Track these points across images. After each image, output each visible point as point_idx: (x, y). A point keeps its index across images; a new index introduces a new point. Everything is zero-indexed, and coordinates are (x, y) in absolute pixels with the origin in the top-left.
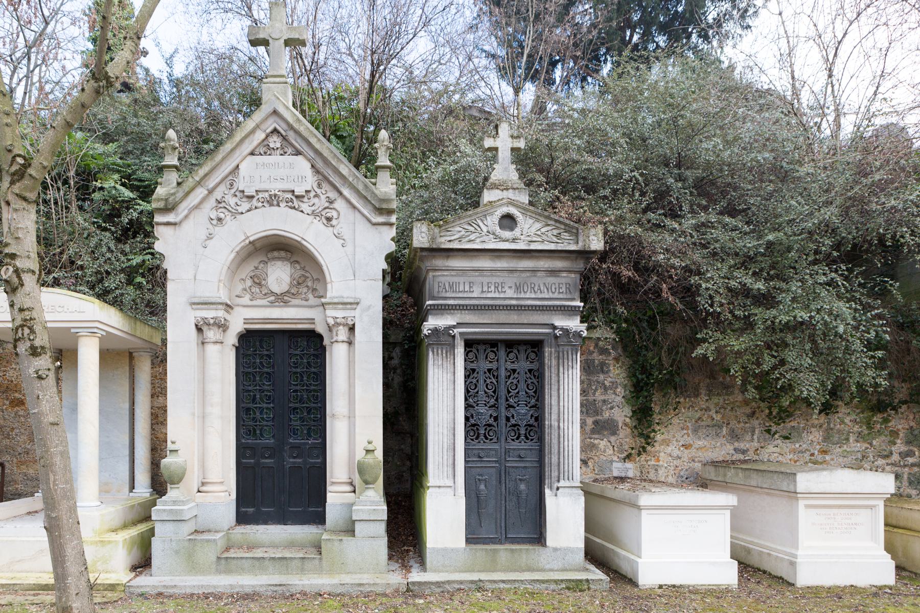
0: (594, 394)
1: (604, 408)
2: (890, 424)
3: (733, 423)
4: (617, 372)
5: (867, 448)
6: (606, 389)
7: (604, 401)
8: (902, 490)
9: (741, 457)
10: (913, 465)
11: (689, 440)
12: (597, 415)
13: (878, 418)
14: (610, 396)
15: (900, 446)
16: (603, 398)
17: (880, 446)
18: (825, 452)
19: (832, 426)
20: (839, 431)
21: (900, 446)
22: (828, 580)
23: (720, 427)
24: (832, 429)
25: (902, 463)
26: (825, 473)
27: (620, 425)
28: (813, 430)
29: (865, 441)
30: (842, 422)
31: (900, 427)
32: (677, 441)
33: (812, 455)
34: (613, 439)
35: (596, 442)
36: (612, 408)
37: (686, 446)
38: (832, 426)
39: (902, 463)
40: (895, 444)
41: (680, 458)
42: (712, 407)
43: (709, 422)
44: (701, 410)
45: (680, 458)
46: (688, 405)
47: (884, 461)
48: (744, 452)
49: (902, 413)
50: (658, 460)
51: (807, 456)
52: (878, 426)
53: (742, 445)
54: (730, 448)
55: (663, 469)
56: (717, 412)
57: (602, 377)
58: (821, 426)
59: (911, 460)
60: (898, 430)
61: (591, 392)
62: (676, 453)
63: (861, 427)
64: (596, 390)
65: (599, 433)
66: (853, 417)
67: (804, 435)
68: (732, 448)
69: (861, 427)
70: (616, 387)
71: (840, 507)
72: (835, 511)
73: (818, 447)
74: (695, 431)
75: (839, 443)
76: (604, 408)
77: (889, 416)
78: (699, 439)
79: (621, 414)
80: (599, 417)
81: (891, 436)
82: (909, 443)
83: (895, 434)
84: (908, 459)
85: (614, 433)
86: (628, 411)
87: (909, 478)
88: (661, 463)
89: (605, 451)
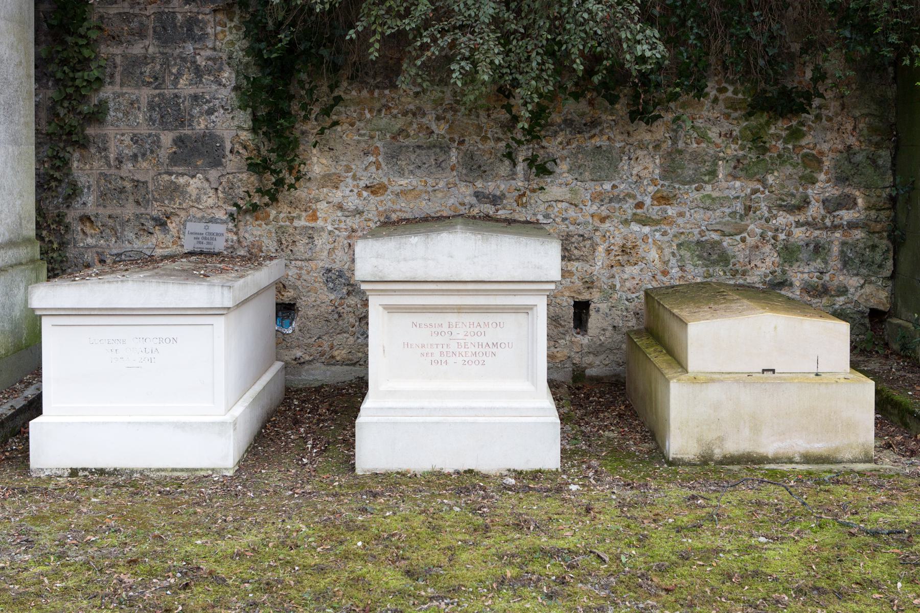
0: (175, 83)
1: (196, 111)
2: (803, 142)
3: (472, 140)
4: (229, 38)
5: (755, 191)
6: (199, 72)
7: (195, 98)
8: (827, 277)
9: (489, 209)
10: (852, 225)
11: (379, 176)
12: (182, 125)
13: (779, 128)
14: (208, 87)
15: (823, 187)
16: (192, 90)
17: (783, 186)
18: (663, 199)
19: (681, 145)
20: (695, 156)
21: (823, 187)
22: (420, 461)
23: (445, 149)
24: (680, 152)
25: (828, 222)
26: (414, 240)
27: (228, 146)
28: (640, 153)
29: (750, 177)
30: (703, 137)
31: (825, 147)
32: (354, 177)
33: (640, 205)
34: (213, 174)
35: (181, 180)
36: (210, 112)
37: (375, 189)
38: (681, 145)
39: (828, 222)
40: (813, 181)
41: (360, 213)
42: (428, 107)
43: (422, 139)
44: (405, 114)
45: (360, 213)
46: (377, 105)
47: (791, 219)
48: (495, 200)
49: (830, 119)
50: (314, 218)
51: (628, 207)
52: (780, 145)
53: (491, 187)
54: (465, 192)
55: (325, 235)
56: (438, 118)
57: (190, 48)
58: (657, 147)
59: (847, 215)
60: (822, 153)
61: (169, 80)
62: (353, 202)
63: (742, 148)
64: (179, 75)
65: (186, 162)
66: (726, 126)
67: (624, 165)
69: (742, 148)
70: (220, 70)
71: (45, 309)
72: (452, 318)
73: (651, 189)
75: (696, 181)
76: (196, 111)
77: (802, 124)
78: (401, 173)
79: (231, 127)
80: (187, 131)
81: (805, 166)
82: (842, 179)
83: (813, 161)
84: (843, 213)
85: (216, 162)
86: (244, 118)
87: (842, 252)
88: (320, 223)
89: (198, 200)
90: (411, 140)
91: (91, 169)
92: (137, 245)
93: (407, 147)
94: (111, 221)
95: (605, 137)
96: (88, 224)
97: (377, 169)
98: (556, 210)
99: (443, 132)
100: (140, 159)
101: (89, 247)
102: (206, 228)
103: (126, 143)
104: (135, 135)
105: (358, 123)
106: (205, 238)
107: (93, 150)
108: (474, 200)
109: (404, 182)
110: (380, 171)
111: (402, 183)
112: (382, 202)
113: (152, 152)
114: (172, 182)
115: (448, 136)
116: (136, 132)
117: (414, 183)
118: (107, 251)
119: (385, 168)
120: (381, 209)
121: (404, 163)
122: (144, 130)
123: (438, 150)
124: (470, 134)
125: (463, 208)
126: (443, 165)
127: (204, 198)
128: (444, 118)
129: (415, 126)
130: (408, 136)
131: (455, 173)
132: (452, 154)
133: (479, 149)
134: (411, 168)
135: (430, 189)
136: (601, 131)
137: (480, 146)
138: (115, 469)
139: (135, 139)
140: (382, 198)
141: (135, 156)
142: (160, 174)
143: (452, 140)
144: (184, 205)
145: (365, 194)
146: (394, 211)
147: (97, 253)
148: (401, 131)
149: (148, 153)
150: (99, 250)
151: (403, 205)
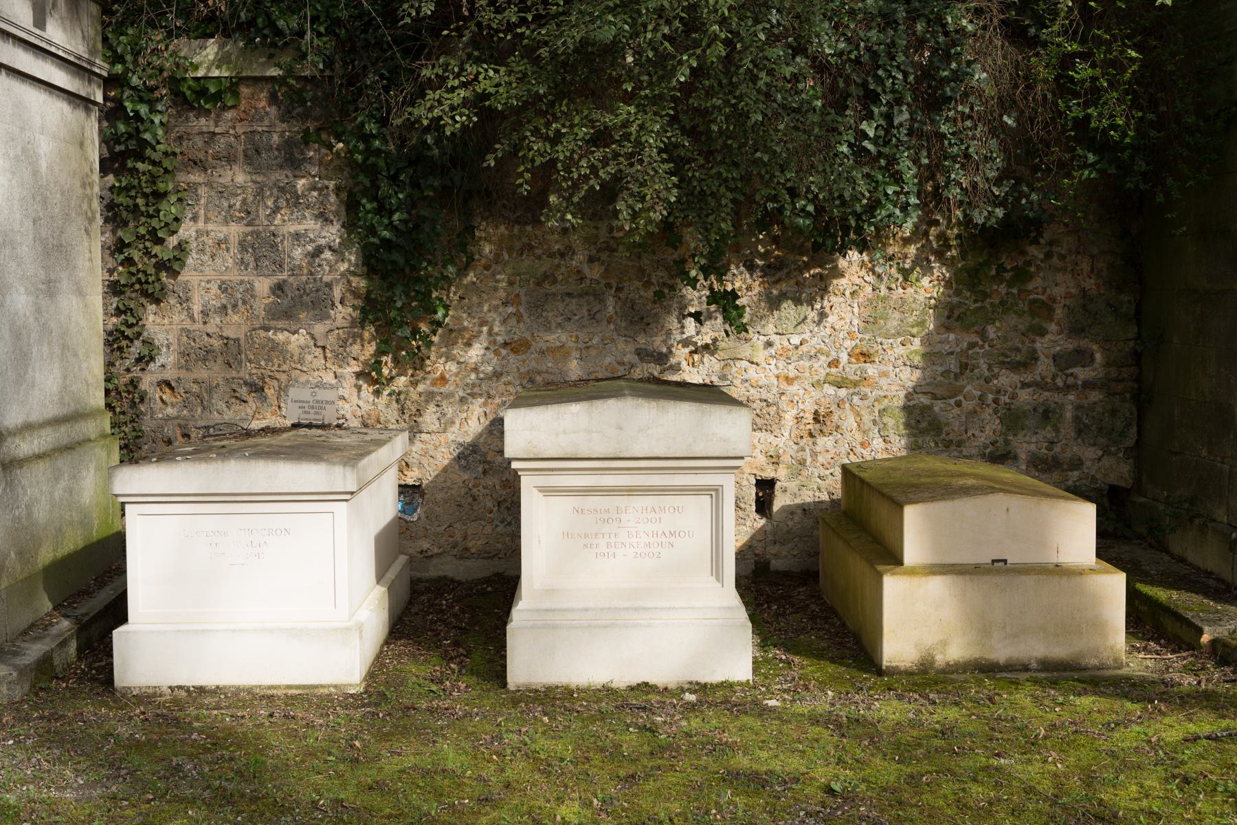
2: (1030, 286)
7: (297, 236)
8: (1057, 449)
10: (1088, 385)
21: (1053, 341)
23: (599, 298)
25: (1060, 382)
29: (967, 329)
31: (1058, 291)
33: (834, 363)
34: (319, 328)
35: (281, 337)
39: (1060, 382)
40: (1042, 333)
44: (551, 255)
46: (518, 245)
49: (1062, 257)
54: (624, 349)
56: (591, 260)
60: (1054, 300)
65: (288, 314)
68: (630, 348)
73: (849, 344)
74: (537, 306)
78: (548, 329)
81: (1033, 314)
82: (1076, 330)
83: (1044, 309)
87: (1077, 419)
89: (301, 361)
90: (558, 286)
91: (171, 323)
92: (229, 415)
93: (554, 295)
94: (195, 386)
95: (792, 282)
96: (167, 390)
97: (518, 322)
98: (734, 369)
99: (597, 277)
100: (230, 311)
101: (169, 418)
102: (314, 394)
103: (213, 292)
104: (223, 282)
105: (494, 266)
106: (312, 407)
107: (172, 301)
108: (635, 359)
109: (551, 337)
110: (522, 325)
111: (548, 338)
112: (524, 361)
113: (244, 302)
114: (269, 339)
115: (603, 282)
116: (224, 278)
117: (564, 338)
118: (191, 424)
119: (528, 321)
120: (522, 370)
121: (550, 314)
122: (234, 277)
123: (591, 298)
124: (630, 280)
125: (622, 368)
126: (598, 316)
127: (309, 358)
128: (599, 259)
129: (563, 269)
130: (555, 281)
131: (612, 327)
132: (608, 303)
133: (641, 297)
134: (559, 320)
135: (581, 345)
136: (788, 274)
137: (642, 293)
138: (218, 687)
139: (224, 288)
140: (524, 357)
141: (224, 307)
142: (254, 329)
143: (609, 286)
144: (285, 367)
145: (504, 352)
146: (539, 373)
147: (180, 426)
148: (545, 277)
149: (240, 302)
150: (183, 422)
151: (550, 365)
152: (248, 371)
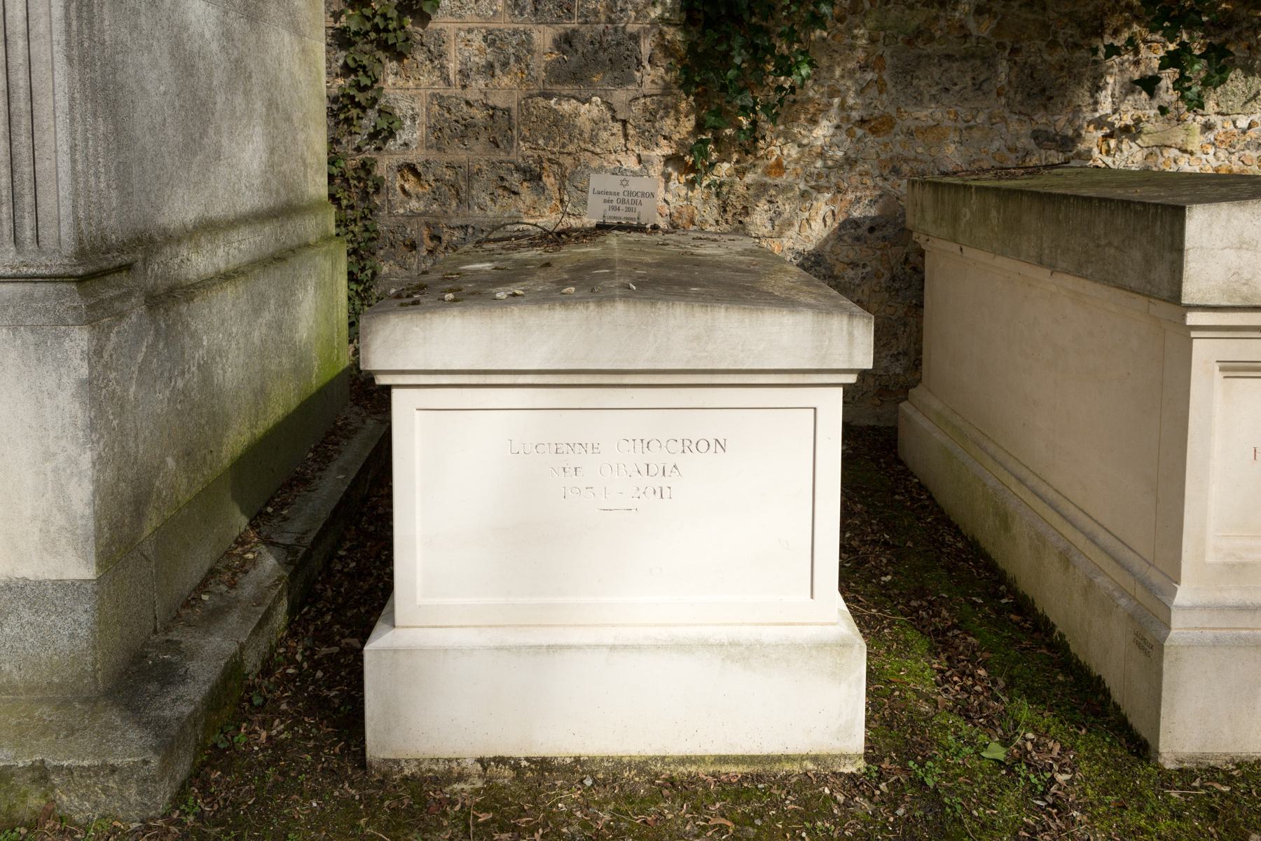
23: (989, 62)
34: (620, 96)
35: (567, 107)
54: (1019, 131)
68: (1026, 129)
74: (906, 73)
78: (918, 101)
89: (594, 139)
90: (936, 46)
91: (418, 87)
92: (494, 211)
93: (929, 56)
94: (449, 172)
95: (1243, 45)
96: (411, 177)
97: (881, 92)
98: (1161, 160)
99: (985, 34)
100: (498, 72)
101: (413, 215)
102: (624, 183)
103: (476, 45)
104: (490, 32)
105: (849, 17)
106: (623, 201)
107: (420, 56)
108: (1031, 144)
109: (922, 114)
110: (885, 96)
111: (919, 114)
112: (886, 145)
113: (518, 59)
114: (550, 109)
115: (994, 41)
116: (491, 26)
117: (938, 115)
118: (443, 222)
119: (893, 91)
120: (883, 157)
121: (922, 83)
122: (505, 24)
123: (978, 62)
124: (1030, 38)
125: (1013, 156)
126: (985, 86)
127: (604, 135)
128: (989, 11)
129: (942, 23)
130: (932, 39)
131: (1003, 101)
132: (1000, 69)
133: (1044, 61)
134: (933, 92)
135: (961, 125)
136: (1238, 35)
137: (1046, 56)
138: (577, 760)
139: (491, 39)
140: (886, 139)
141: (491, 66)
142: (531, 96)
143: (1001, 46)
144: (571, 148)
145: (859, 132)
146: (906, 160)
147: (428, 225)
148: (919, 33)
149: (512, 60)
150: (431, 220)
151: (920, 150)
152: (523, 151)
